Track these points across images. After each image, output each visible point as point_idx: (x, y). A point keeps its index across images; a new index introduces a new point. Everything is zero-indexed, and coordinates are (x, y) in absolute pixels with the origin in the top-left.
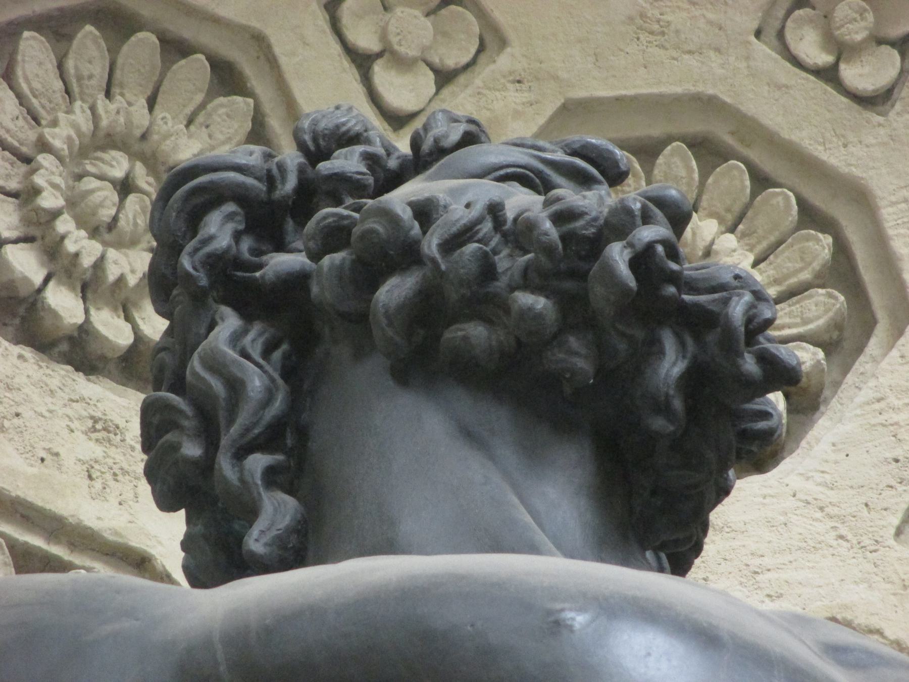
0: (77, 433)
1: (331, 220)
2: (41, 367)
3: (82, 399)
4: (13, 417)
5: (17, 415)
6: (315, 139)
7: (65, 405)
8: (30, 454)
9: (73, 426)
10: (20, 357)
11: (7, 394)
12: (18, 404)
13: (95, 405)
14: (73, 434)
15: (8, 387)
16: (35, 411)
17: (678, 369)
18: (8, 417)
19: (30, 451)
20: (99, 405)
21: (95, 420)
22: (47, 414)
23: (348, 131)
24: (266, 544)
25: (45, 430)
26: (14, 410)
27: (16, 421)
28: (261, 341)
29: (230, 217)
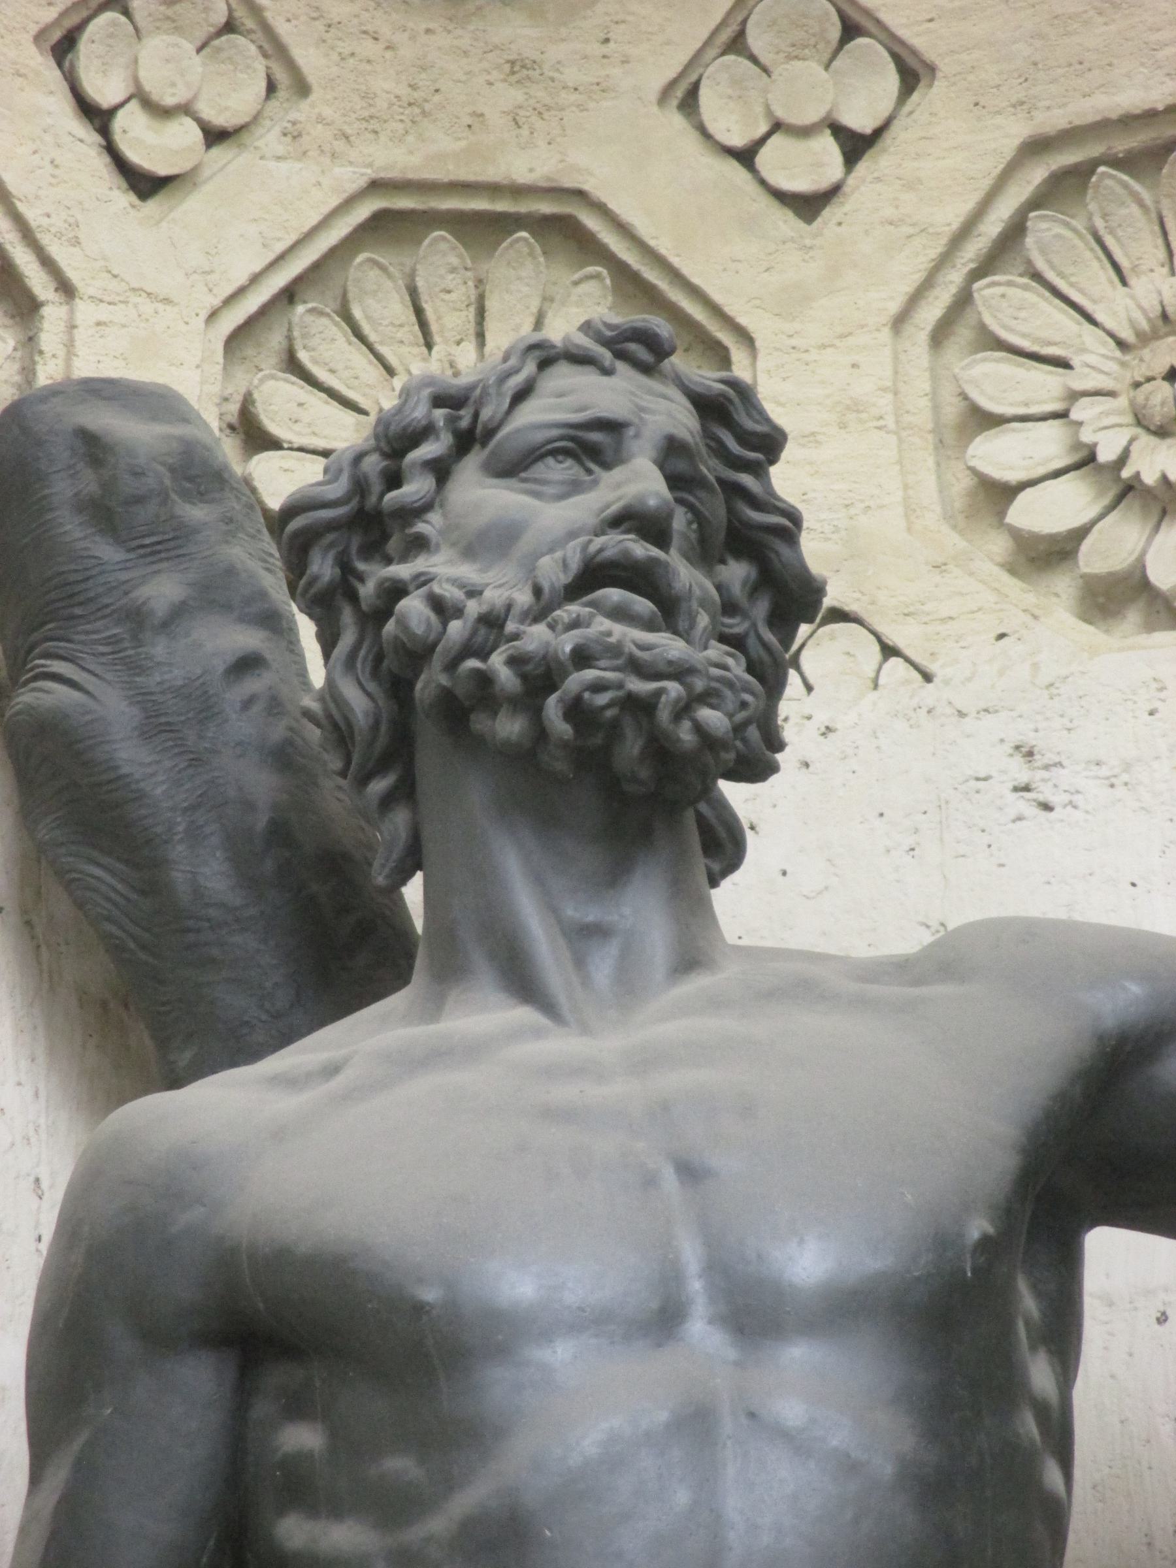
0: (500, 85)
1: (387, 584)
2: (449, 32)
3: (496, 47)
4: (433, 95)
5: (437, 91)
6: (389, 442)
7: (481, 60)
8: (457, 125)
9: (490, 78)
10: (428, 31)
11: (423, 76)
12: (435, 81)
13: (510, 49)
14: (493, 87)
15: (422, 68)
16: (454, 81)
17: (636, 751)
18: (429, 99)
19: (455, 123)
20: (512, 46)
21: (513, 63)
22: (464, 78)
23: (414, 430)
24: (387, 877)
25: (466, 95)
26: (432, 88)
27: (437, 98)
28: (371, 657)
29: (331, 545)
